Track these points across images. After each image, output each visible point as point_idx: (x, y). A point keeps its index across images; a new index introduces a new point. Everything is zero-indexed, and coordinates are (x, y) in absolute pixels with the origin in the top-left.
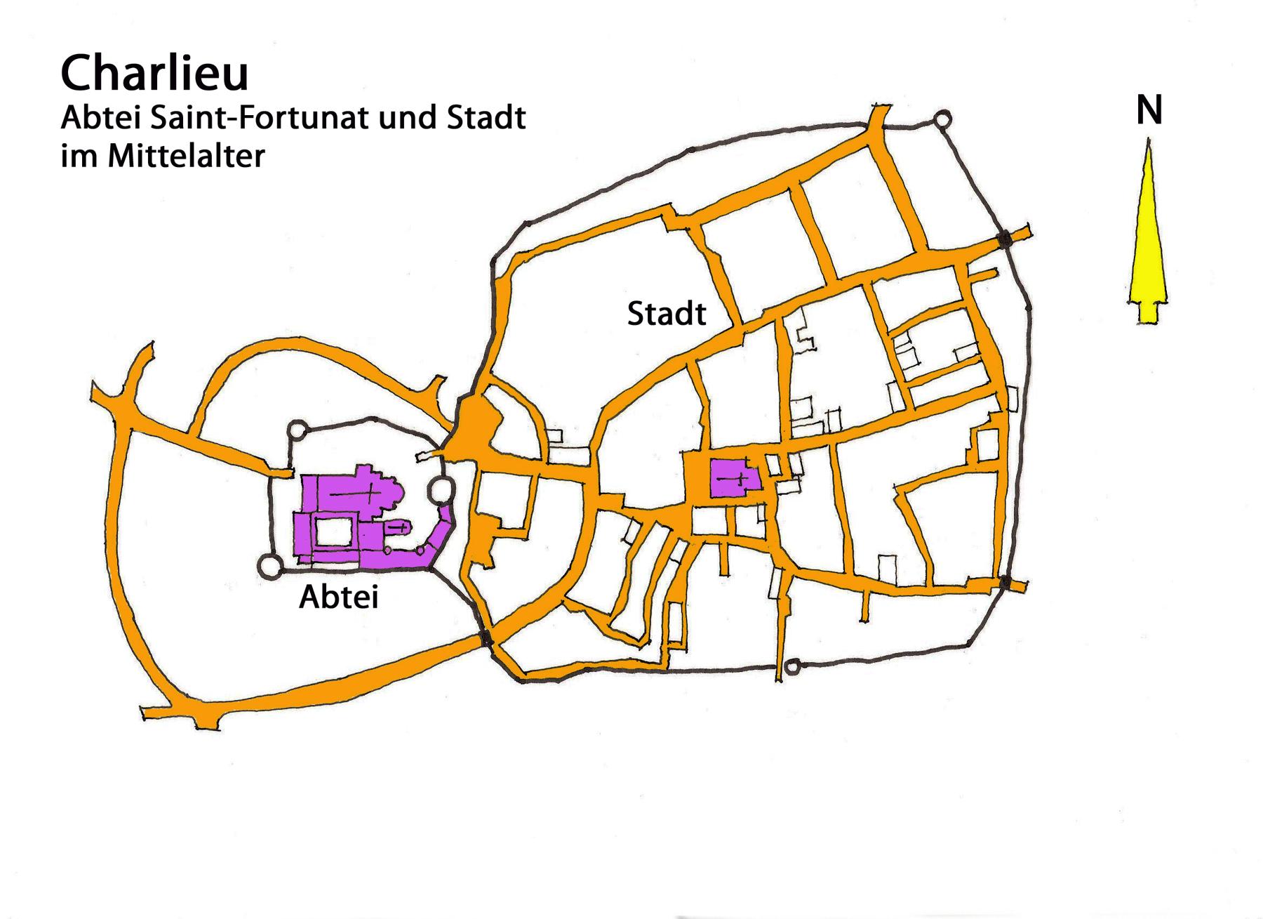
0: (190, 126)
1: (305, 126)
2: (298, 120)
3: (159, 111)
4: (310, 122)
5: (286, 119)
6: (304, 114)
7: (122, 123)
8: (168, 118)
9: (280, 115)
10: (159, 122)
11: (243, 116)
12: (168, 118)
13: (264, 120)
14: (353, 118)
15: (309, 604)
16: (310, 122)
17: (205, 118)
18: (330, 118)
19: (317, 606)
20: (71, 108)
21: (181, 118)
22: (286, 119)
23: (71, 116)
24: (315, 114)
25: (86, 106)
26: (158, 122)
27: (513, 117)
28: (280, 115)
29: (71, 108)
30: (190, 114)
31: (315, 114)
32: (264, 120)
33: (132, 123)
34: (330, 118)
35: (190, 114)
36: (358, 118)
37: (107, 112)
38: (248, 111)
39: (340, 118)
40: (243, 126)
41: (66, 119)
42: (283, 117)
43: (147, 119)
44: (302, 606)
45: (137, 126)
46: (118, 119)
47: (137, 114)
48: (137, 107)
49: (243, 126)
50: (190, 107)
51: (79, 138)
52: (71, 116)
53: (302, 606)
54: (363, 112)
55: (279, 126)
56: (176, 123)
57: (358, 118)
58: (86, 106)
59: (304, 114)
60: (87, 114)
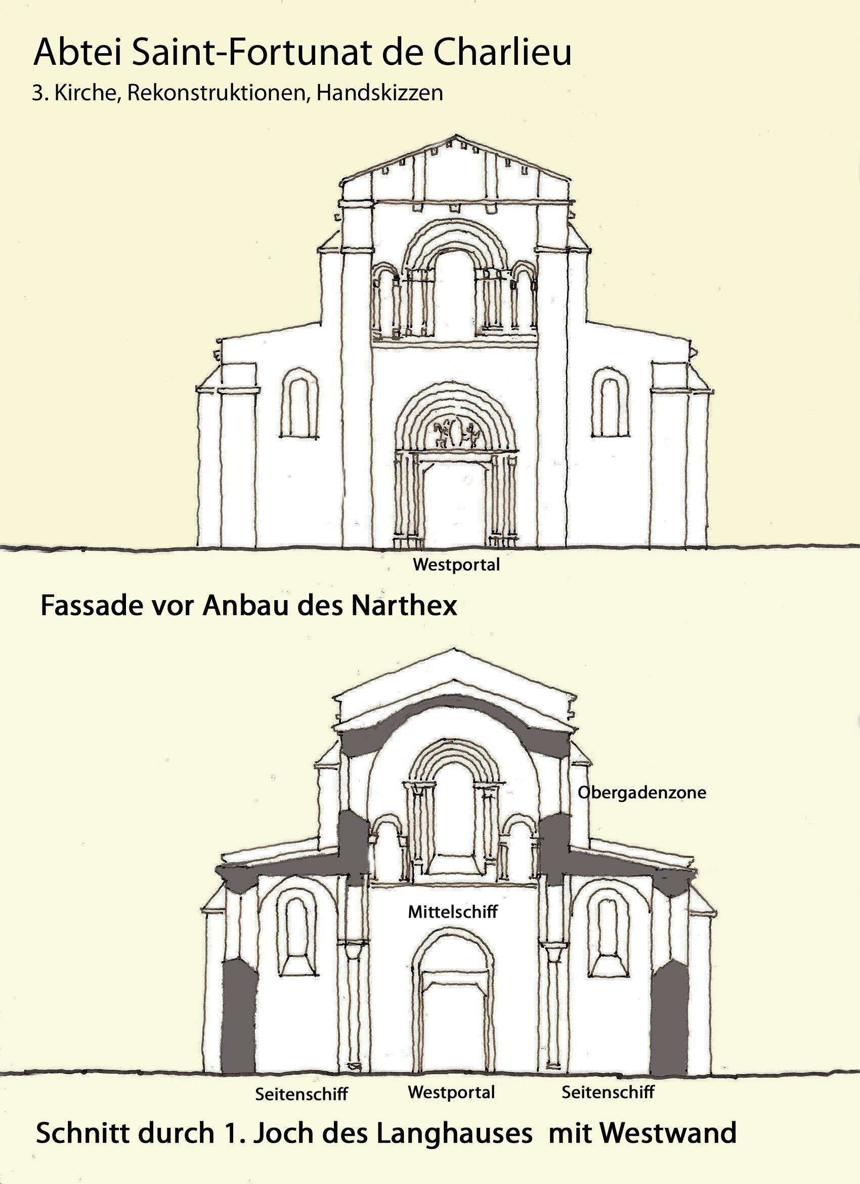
2: (294, 53)
3: (140, 44)
4: (307, 57)
5: (281, 54)
7: (101, 58)
10: (142, 57)
11: (233, 51)
13: (257, 55)
15: (212, 611)
16: (307, 57)
17: (191, 53)
18: (329, 53)
19: (218, 613)
22: (281, 54)
30: (175, 47)
32: (257, 55)
34: (329, 53)
35: (175, 47)
36: (360, 52)
37: (86, 46)
38: (238, 45)
39: (341, 53)
41: (39, 54)
43: (129, 54)
44: (205, 613)
45: (118, 63)
47: (118, 47)
48: (118, 40)
51: (50, 74)
53: (205, 613)
57: (360, 52)
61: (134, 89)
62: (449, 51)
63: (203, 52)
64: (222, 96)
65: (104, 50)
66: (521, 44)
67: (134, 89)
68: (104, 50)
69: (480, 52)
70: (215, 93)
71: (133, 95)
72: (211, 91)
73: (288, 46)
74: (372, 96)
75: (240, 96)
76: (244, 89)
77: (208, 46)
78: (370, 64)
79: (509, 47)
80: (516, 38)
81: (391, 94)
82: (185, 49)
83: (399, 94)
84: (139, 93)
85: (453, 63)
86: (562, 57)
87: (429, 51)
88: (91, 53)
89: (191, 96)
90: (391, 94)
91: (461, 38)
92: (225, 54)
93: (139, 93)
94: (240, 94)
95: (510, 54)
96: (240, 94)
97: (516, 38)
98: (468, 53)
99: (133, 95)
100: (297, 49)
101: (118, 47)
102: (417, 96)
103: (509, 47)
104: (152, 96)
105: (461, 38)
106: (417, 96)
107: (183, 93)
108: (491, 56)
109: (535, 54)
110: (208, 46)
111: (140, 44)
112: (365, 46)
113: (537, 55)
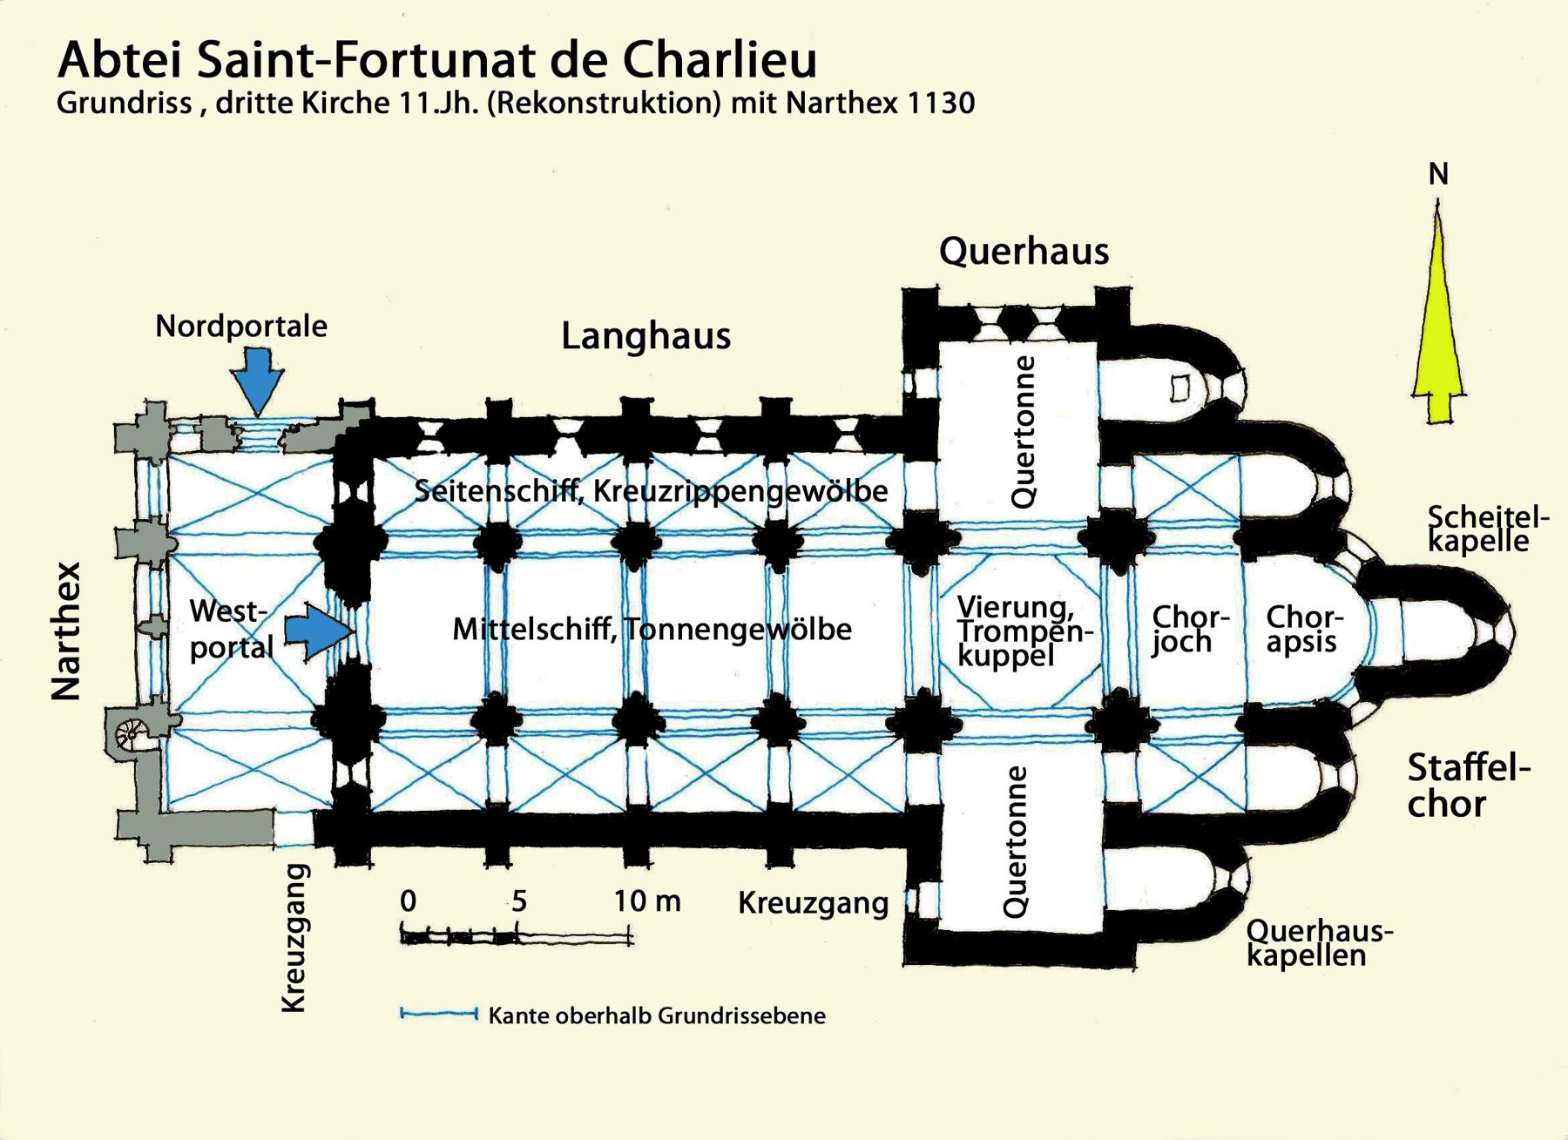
0: (258, 74)
1: (437, 73)
2: (426, 63)
3: (210, 50)
4: (444, 66)
5: (407, 63)
6: (435, 54)
8: (225, 61)
10: (210, 67)
11: (341, 59)
12: (225, 61)
13: (374, 64)
16: (444, 66)
17: (281, 62)
18: (475, 62)
20: (74, 46)
21: (244, 61)
22: (407, 63)
23: (73, 58)
24: (452, 54)
25: (98, 42)
26: (209, 67)
27: (566, 324)
28: (397, 56)
29: (74, 46)
30: (258, 54)
31: (452, 54)
32: (374, 64)
33: (168, 69)
34: (475, 62)
35: (258, 54)
37: (130, 52)
38: (348, 51)
39: (492, 60)
40: (340, 73)
41: (66, 63)
42: (403, 60)
43: (192, 62)
45: (176, 73)
47: (176, 54)
48: (176, 44)
49: (340, 73)
50: (258, 44)
52: (73, 58)
54: (526, 52)
55: (396, 74)
56: (237, 69)
58: (98, 42)
59: (435, 54)
60: (99, 55)
61: (505, 97)
62: (645, 59)
63: (297, 60)
64: (630, 107)
66: (746, 50)
67: (505, 97)
69: (687, 60)
70: (619, 104)
71: (505, 107)
72: (615, 100)
73: (417, 52)
75: (656, 108)
76: (661, 98)
77: (304, 52)
78: (533, 75)
79: (728, 53)
80: (739, 42)
82: (273, 56)
84: (514, 103)
85: (650, 74)
86: (803, 66)
88: (138, 62)
89: (586, 107)
91: (662, 42)
92: (328, 62)
93: (514, 103)
94: (655, 104)
95: (730, 62)
96: (655, 104)
97: (739, 42)
98: (670, 62)
99: (505, 107)
100: (430, 55)
101: (176, 54)
103: (728, 53)
104: (531, 108)
105: (662, 42)
107: (575, 104)
109: (766, 63)
110: (304, 52)
111: (210, 50)
112: (526, 52)
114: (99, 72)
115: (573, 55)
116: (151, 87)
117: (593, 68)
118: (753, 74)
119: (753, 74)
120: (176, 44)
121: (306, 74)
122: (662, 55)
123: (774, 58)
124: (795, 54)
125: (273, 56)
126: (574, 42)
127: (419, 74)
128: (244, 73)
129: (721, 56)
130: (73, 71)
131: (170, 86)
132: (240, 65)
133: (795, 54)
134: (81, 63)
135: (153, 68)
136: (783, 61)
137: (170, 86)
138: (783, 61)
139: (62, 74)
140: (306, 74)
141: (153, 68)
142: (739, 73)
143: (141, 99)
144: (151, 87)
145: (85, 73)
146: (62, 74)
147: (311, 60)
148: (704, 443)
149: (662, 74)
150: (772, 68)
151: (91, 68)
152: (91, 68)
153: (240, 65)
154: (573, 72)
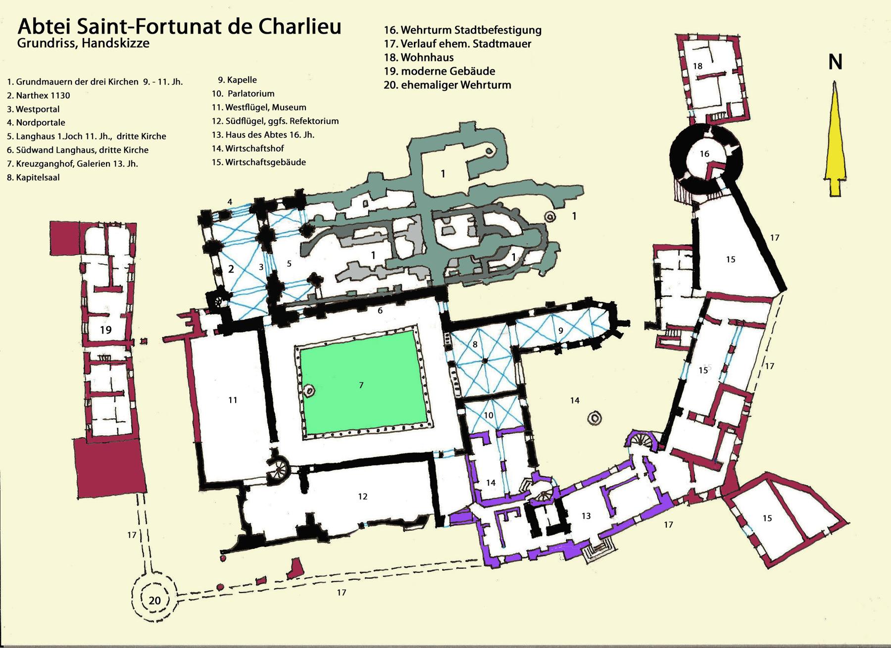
0: (103, 32)
1: (179, 32)
2: (175, 27)
3: (83, 22)
4: (182, 29)
5: (167, 28)
6: (179, 24)
8: (89, 27)
9: (163, 25)
10: (83, 30)
11: (138, 26)
12: (89, 27)
14: (211, 27)
16: (182, 29)
17: (113, 27)
18: (196, 27)
20: (24, 20)
21: (97, 27)
22: (167, 28)
23: (24, 26)
25: (35, 19)
28: (163, 25)
29: (24, 20)
30: (103, 24)
33: (65, 30)
34: (196, 27)
35: (103, 24)
36: (214, 27)
37: (49, 23)
38: (141, 23)
40: (138, 32)
41: (21, 28)
42: (165, 27)
43: (75, 27)
45: (68, 32)
46: (56, 28)
47: (68, 24)
48: (68, 20)
49: (138, 32)
52: (24, 26)
54: (217, 23)
55: (162, 32)
56: (94, 30)
57: (214, 27)
58: (35, 19)
60: (35, 24)
62: (268, 26)
63: (120, 27)
65: (60, 26)
66: (311, 22)
68: (60, 26)
73: (171, 23)
74: (114, 45)
77: (123, 23)
81: (126, 44)
82: (109, 25)
83: (131, 44)
86: (335, 29)
87: (256, 26)
90: (126, 44)
91: (275, 19)
98: (279, 27)
101: (68, 24)
102: (142, 45)
105: (275, 19)
106: (142, 45)
108: (293, 29)
109: (320, 28)
110: (123, 23)
111: (83, 22)
112: (217, 23)
113: (322, 28)
114: (35, 32)
115: (237, 24)
116: (58, 37)
117: (246, 30)
118: (314, 32)
119: (314, 32)
120: (68, 20)
121: (123, 32)
122: (275, 24)
123: (323, 26)
124: (332, 24)
125: (109, 25)
126: (238, 19)
127: (172, 32)
128: (97, 32)
129: (300, 25)
130: (24, 31)
131: (65, 37)
132: (95, 29)
133: (332, 24)
134: (28, 28)
135: (59, 30)
136: (327, 27)
137: (65, 37)
138: (327, 27)
139: (20, 32)
140: (123, 32)
141: (59, 30)
142: (308, 32)
143: (53, 42)
144: (58, 37)
145: (29, 32)
146: (20, 32)
147: (126, 26)
148: (261, 222)
149: (275, 32)
150: (322, 30)
151: (32, 30)
152: (32, 30)
153: (95, 29)
154: (238, 32)
